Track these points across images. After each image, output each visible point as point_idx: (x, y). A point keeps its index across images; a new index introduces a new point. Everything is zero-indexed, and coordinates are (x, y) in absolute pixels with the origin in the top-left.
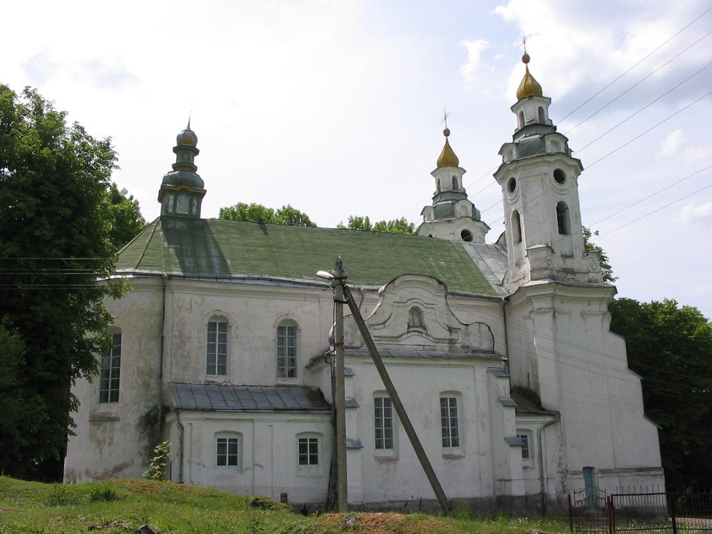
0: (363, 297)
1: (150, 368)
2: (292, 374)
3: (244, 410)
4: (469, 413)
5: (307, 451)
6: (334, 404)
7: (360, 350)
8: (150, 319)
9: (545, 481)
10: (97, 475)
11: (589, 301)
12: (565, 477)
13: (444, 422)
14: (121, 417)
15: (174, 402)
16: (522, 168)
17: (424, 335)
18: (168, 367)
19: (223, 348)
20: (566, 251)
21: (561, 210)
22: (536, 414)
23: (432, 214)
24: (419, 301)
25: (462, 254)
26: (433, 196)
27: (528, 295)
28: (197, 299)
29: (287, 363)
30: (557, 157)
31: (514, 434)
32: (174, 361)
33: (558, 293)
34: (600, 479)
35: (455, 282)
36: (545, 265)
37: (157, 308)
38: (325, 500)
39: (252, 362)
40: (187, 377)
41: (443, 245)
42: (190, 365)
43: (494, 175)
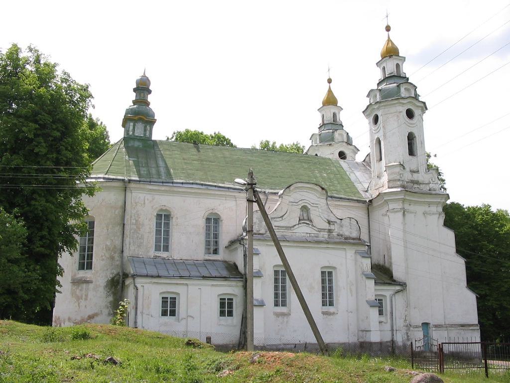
0: (267, 198)
1: (115, 246)
2: (216, 252)
3: (181, 277)
4: (341, 282)
5: (226, 308)
6: (245, 274)
7: (265, 236)
8: (115, 211)
9: (395, 332)
10: (77, 321)
11: (429, 204)
12: (409, 329)
13: (323, 288)
14: (94, 280)
15: (131, 270)
16: (383, 107)
17: (310, 226)
18: (128, 246)
19: (167, 233)
20: (414, 168)
21: (411, 138)
22: (390, 284)
23: (318, 140)
24: (308, 202)
25: (339, 169)
26: (319, 126)
27: (385, 199)
28: (149, 197)
29: (212, 244)
30: (409, 100)
31: (373, 298)
32: (132, 241)
33: (407, 198)
34: (434, 332)
35: (334, 189)
36: (398, 177)
37: (121, 203)
38: (238, 342)
39: (187, 243)
40: (140, 253)
41: (326, 162)
42: (142, 244)
43: (363, 112)
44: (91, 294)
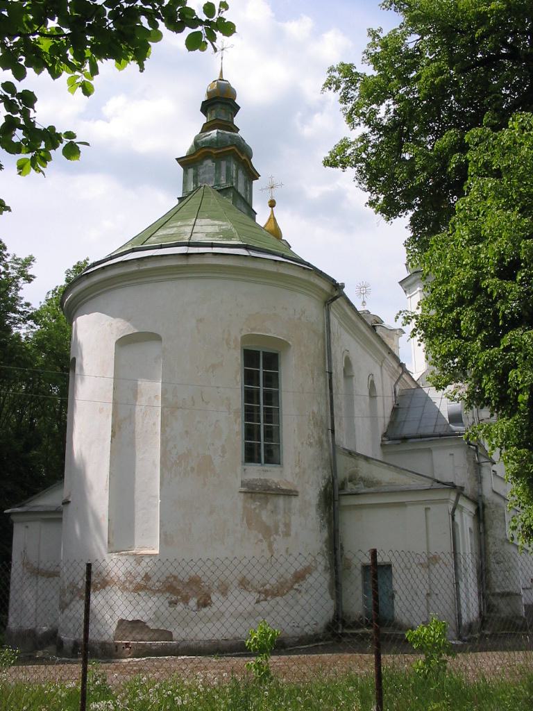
10: (268, 587)
14: (299, 489)
44: (296, 520)
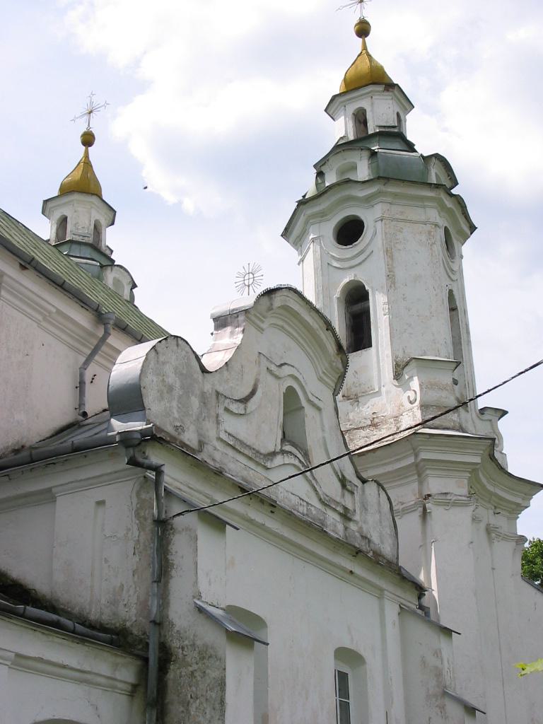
0: (107, 334)
16: (390, 200)
27: (423, 455)
